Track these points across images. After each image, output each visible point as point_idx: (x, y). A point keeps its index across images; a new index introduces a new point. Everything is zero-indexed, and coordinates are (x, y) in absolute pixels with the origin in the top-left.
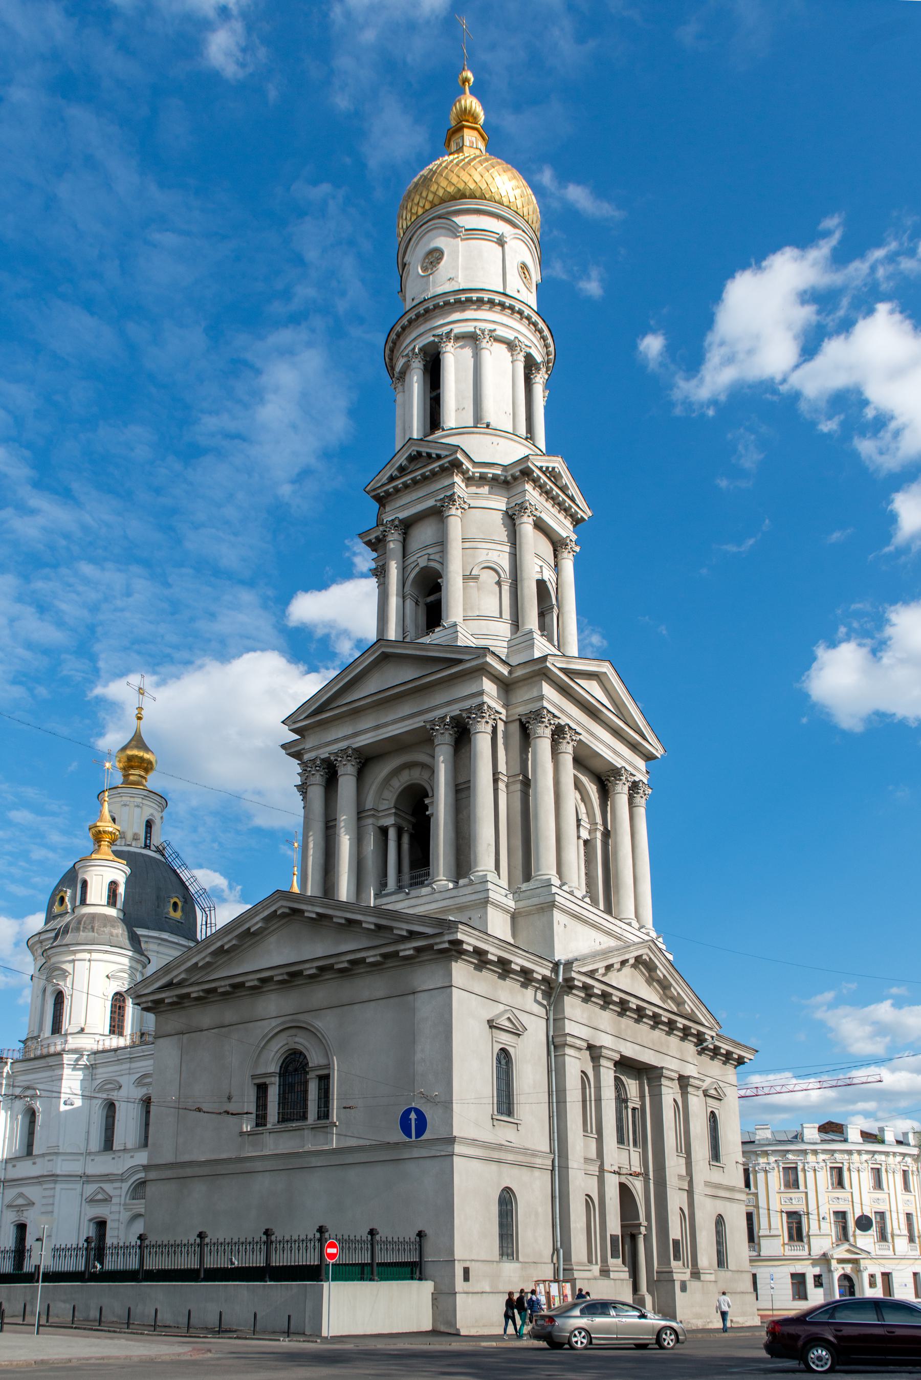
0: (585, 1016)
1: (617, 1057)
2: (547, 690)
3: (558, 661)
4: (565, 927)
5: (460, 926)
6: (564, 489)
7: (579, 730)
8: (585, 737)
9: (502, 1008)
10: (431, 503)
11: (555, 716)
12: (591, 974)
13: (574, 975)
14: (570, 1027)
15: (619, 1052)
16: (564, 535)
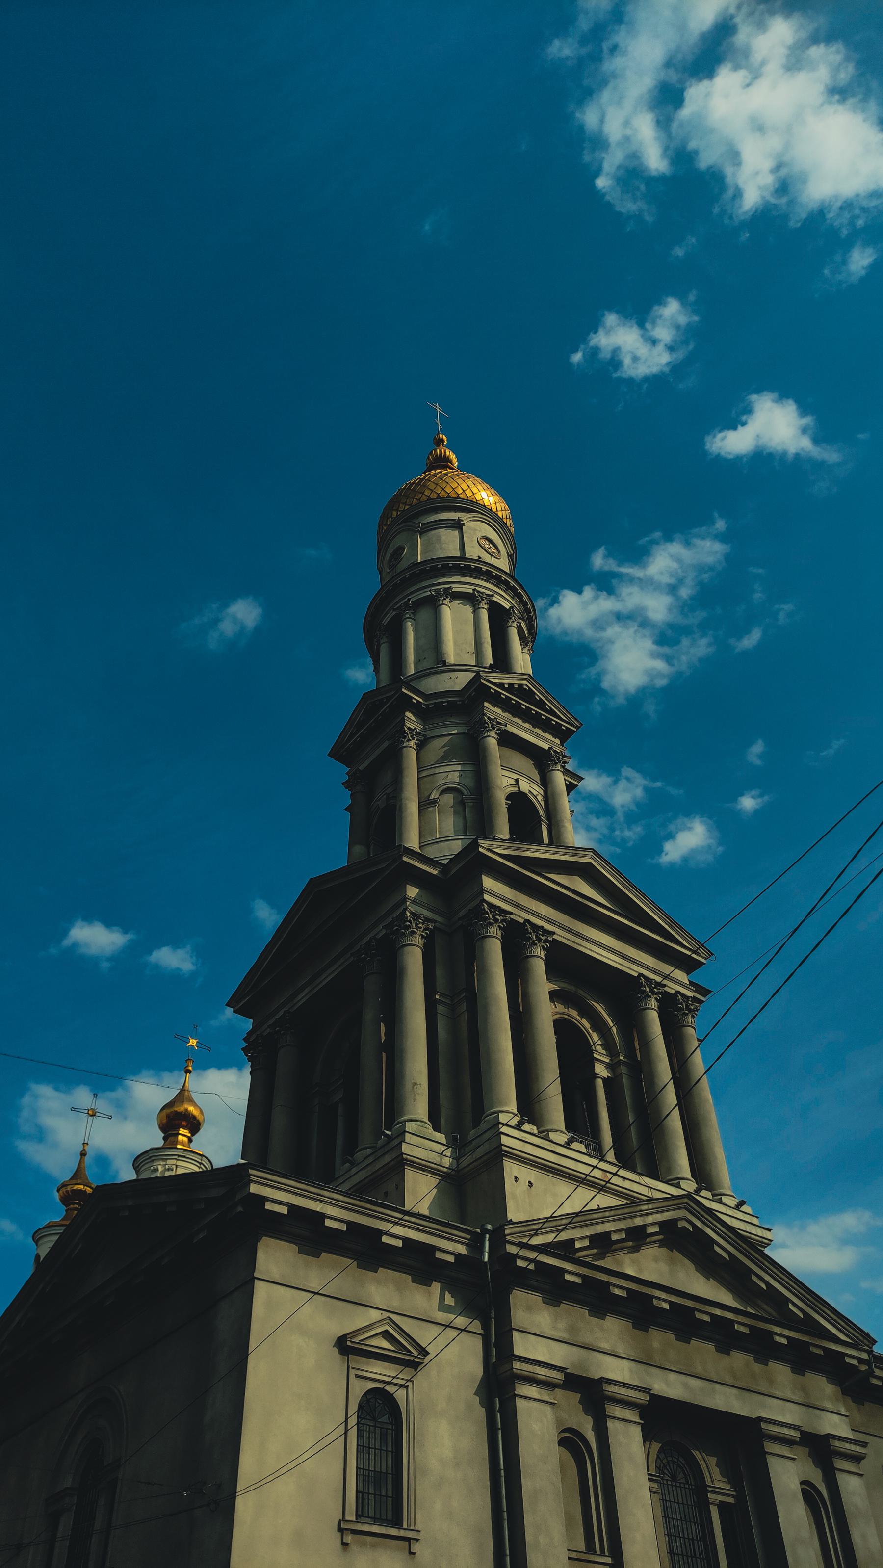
0: (562, 1325)
1: (642, 1398)
2: (488, 882)
3: (500, 847)
4: (530, 1187)
5: (251, 1172)
6: (540, 704)
7: (547, 926)
8: (561, 936)
9: (375, 1315)
10: (386, 744)
11: (503, 911)
12: (565, 1249)
13: (511, 1249)
14: (522, 1346)
15: (647, 1391)
16: (546, 746)
